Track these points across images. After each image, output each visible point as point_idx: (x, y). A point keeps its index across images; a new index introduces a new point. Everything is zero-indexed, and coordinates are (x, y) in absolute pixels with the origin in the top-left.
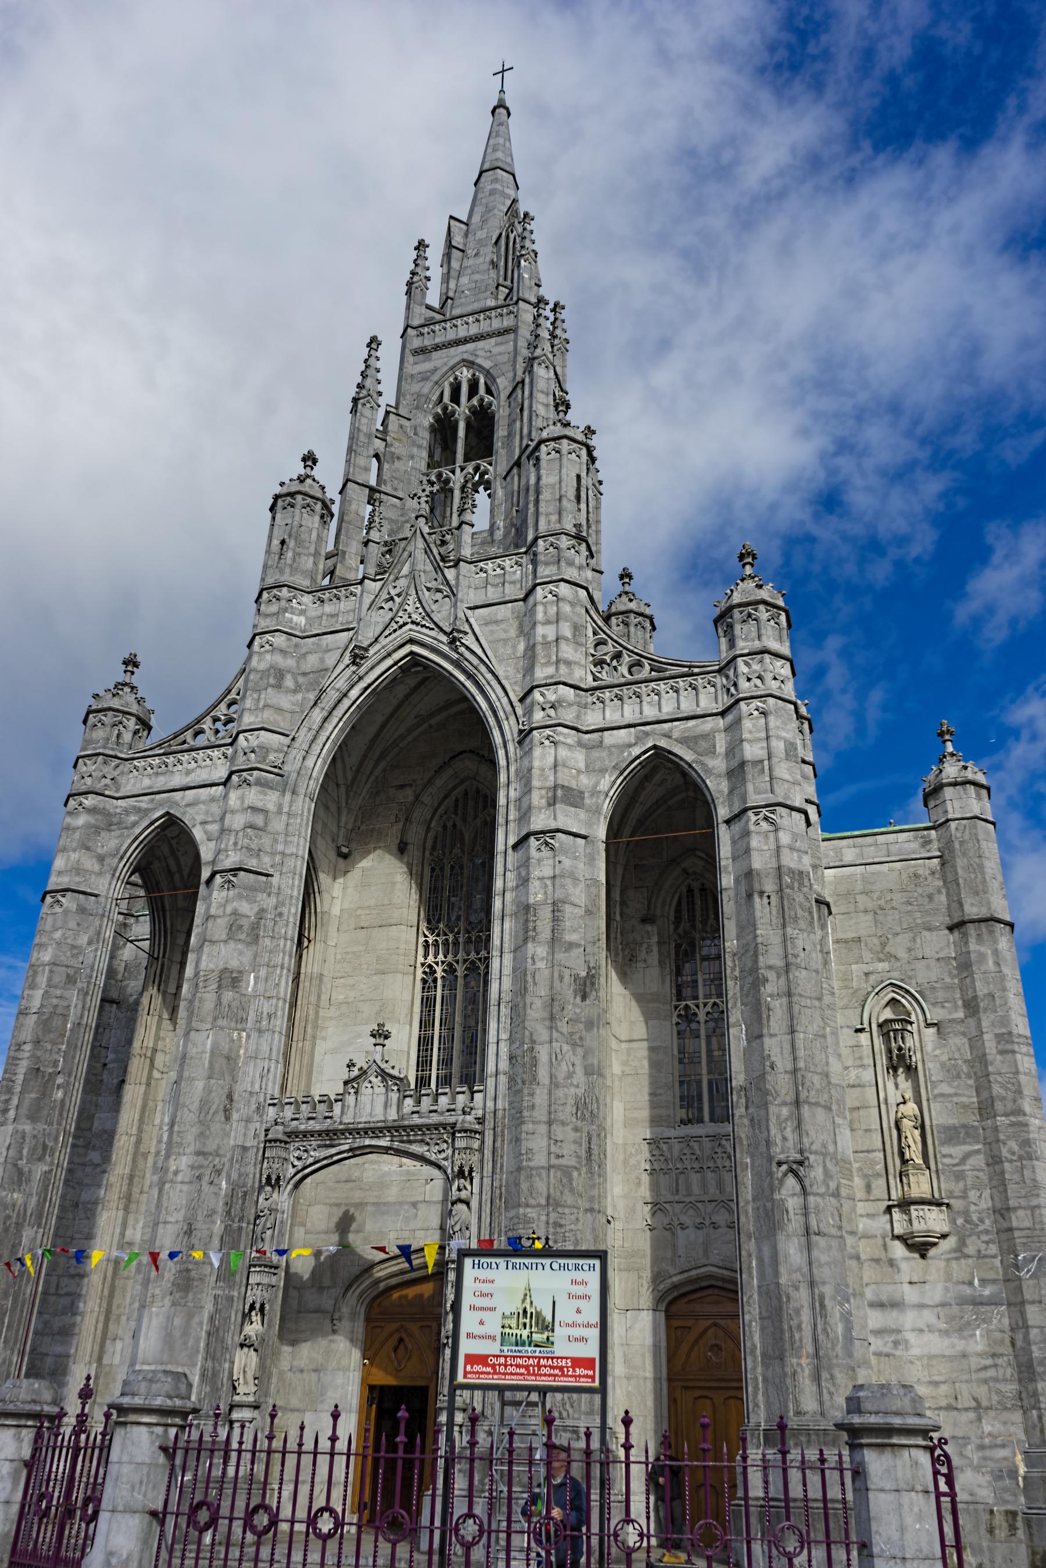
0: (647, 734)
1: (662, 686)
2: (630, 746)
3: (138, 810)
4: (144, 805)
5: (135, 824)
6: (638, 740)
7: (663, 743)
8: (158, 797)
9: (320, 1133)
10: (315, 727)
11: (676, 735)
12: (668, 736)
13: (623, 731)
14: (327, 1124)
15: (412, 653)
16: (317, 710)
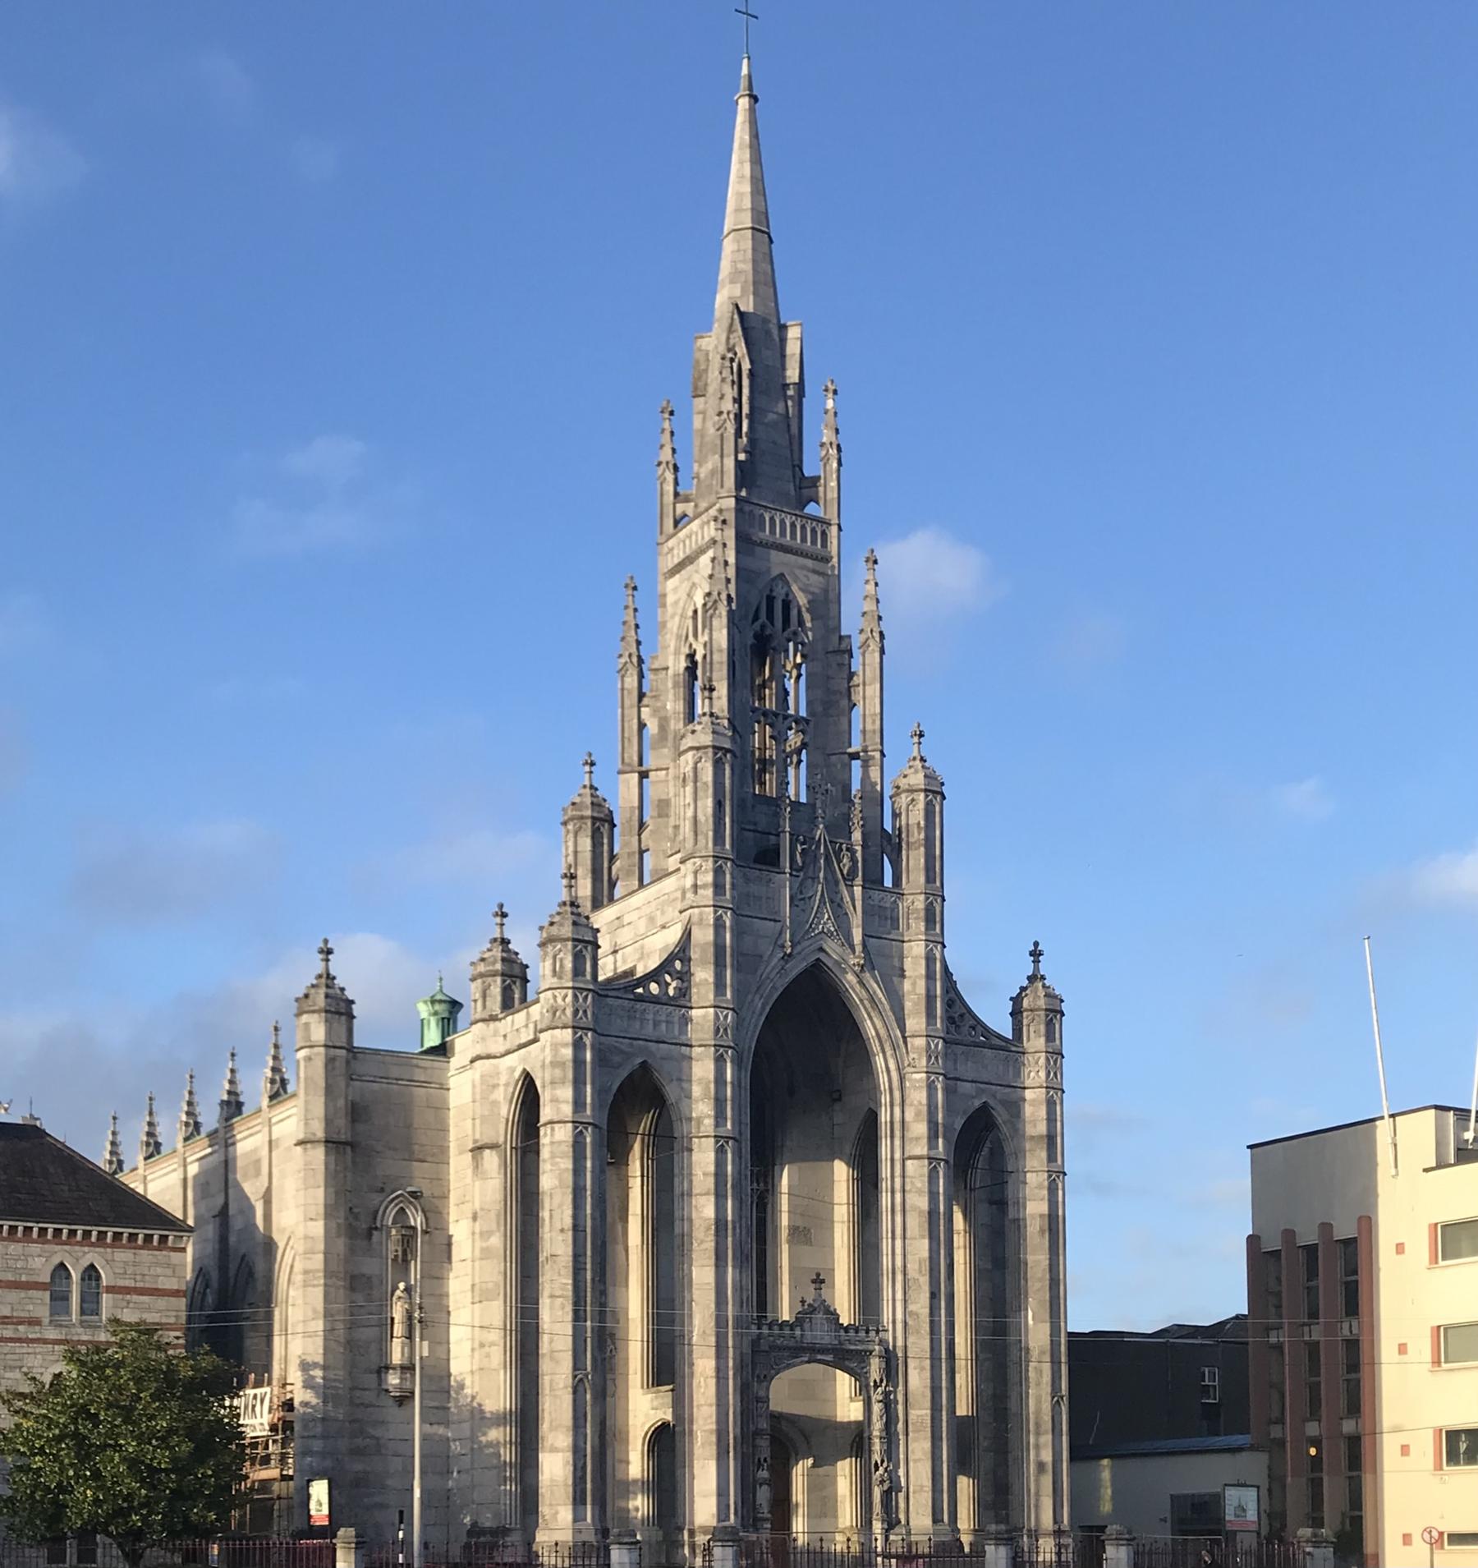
0: (983, 1091)
1: (988, 1052)
2: (973, 1097)
3: (622, 1052)
4: (623, 1047)
5: (620, 1065)
6: (980, 1092)
7: (992, 1102)
8: (635, 1042)
9: (790, 1348)
10: (757, 1012)
11: (999, 1096)
12: (994, 1096)
13: (969, 1084)
14: (792, 1343)
15: (818, 959)
16: (758, 996)
